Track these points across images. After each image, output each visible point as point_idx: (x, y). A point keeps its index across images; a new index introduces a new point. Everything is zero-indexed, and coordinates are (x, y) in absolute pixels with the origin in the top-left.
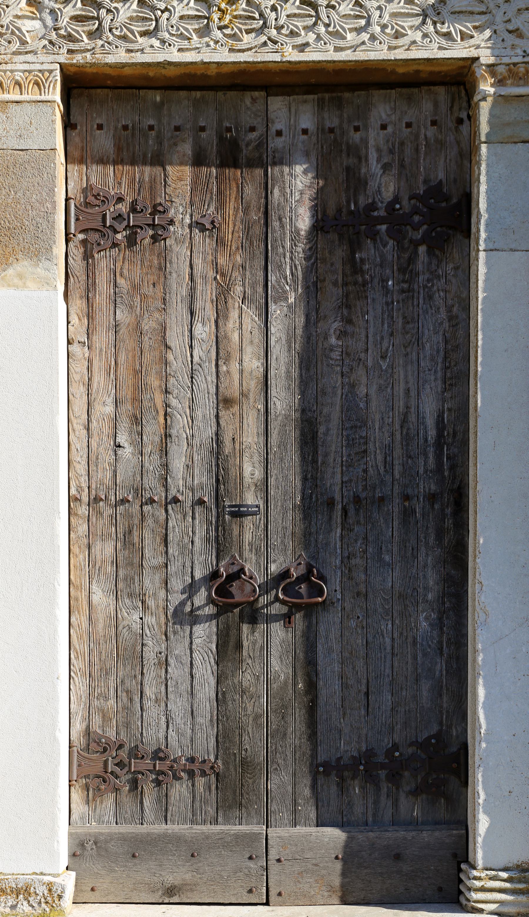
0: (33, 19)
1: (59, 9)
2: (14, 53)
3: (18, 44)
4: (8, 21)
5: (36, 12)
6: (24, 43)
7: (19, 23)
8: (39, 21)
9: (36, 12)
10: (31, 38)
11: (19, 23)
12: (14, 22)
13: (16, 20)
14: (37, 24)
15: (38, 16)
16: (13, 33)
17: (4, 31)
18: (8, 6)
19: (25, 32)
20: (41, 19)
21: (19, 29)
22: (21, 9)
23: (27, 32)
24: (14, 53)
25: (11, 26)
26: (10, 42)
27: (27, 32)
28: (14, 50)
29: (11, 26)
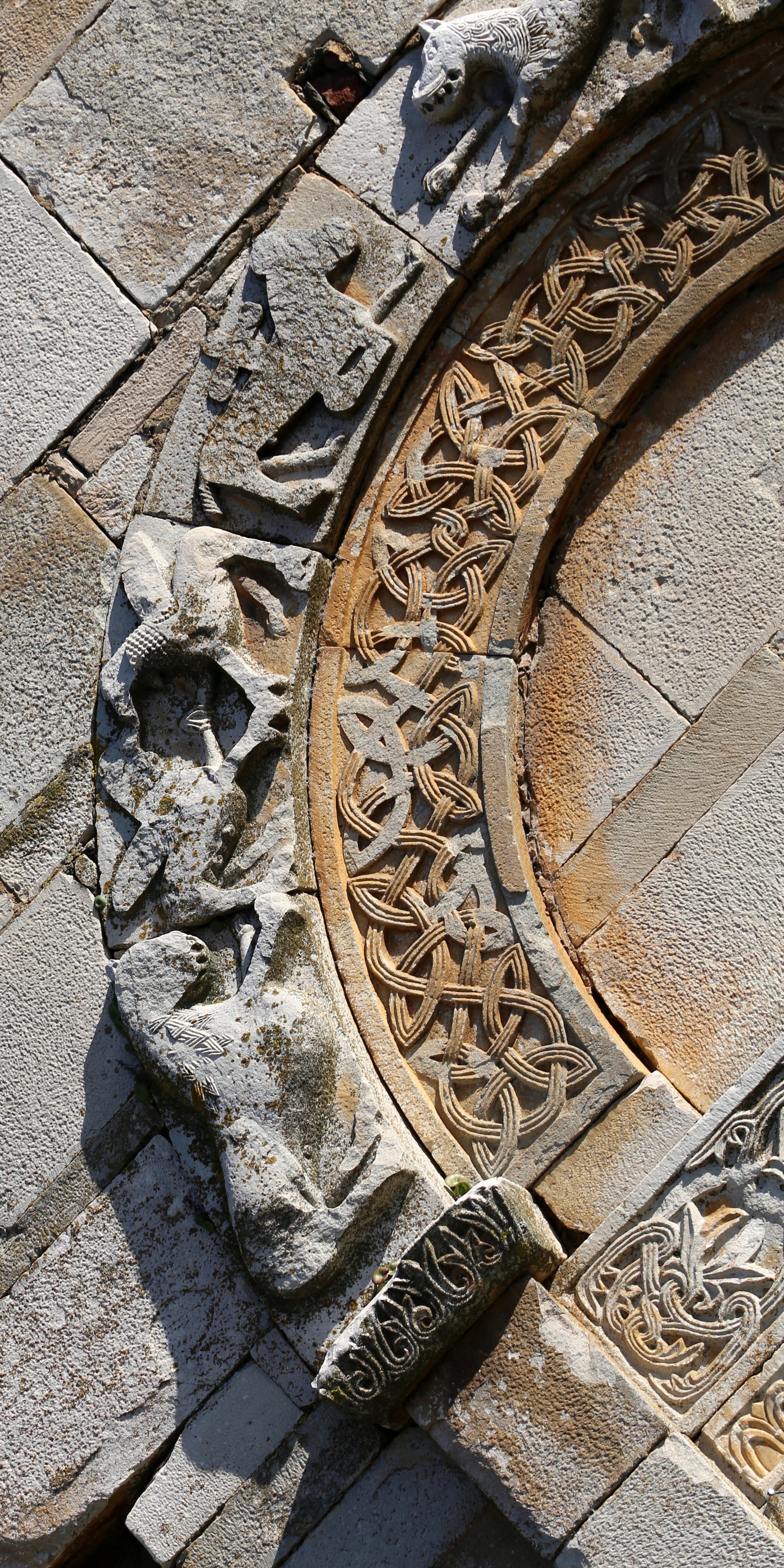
0: (738, 1228)
1: (769, 1164)
2: (765, 1324)
3: (757, 1300)
4: (700, 1276)
5: (732, 1211)
6: (763, 1288)
7: (722, 1260)
8: (753, 1222)
9: (732, 1211)
10: (767, 1265)
11: (722, 1260)
12: (713, 1268)
13: (712, 1262)
14: (755, 1230)
15: (745, 1213)
16: (729, 1290)
17: (711, 1304)
18: (677, 1253)
19: (748, 1267)
20: (753, 1215)
21: (735, 1272)
22: (704, 1234)
23: (751, 1260)
24: (765, 1324)
25: (715, 1282)
26: (739, 1313)
27: (751, 1260)
28: (760, 1316)
29: (715, 1282)
